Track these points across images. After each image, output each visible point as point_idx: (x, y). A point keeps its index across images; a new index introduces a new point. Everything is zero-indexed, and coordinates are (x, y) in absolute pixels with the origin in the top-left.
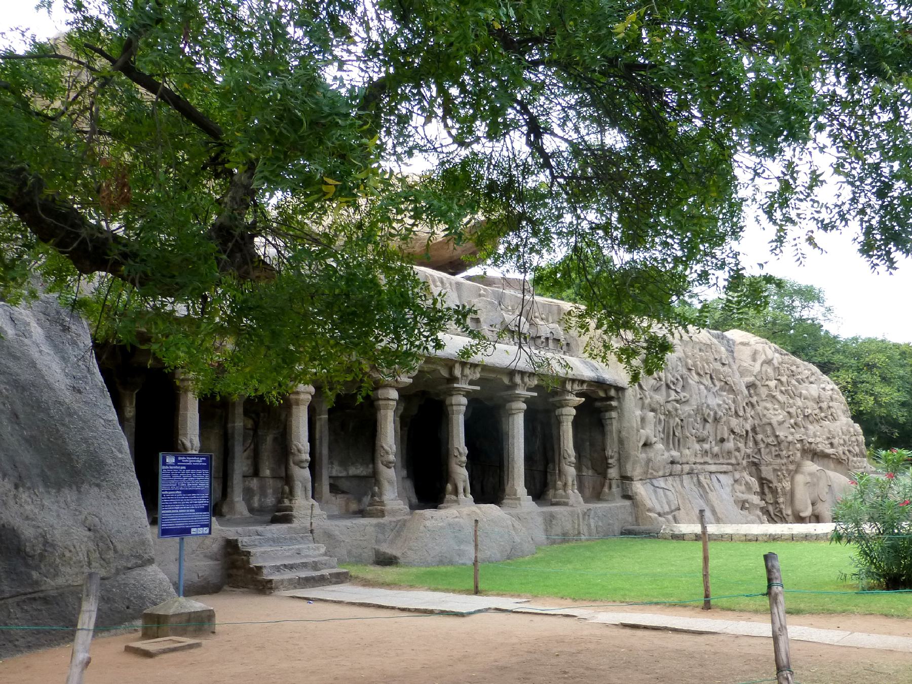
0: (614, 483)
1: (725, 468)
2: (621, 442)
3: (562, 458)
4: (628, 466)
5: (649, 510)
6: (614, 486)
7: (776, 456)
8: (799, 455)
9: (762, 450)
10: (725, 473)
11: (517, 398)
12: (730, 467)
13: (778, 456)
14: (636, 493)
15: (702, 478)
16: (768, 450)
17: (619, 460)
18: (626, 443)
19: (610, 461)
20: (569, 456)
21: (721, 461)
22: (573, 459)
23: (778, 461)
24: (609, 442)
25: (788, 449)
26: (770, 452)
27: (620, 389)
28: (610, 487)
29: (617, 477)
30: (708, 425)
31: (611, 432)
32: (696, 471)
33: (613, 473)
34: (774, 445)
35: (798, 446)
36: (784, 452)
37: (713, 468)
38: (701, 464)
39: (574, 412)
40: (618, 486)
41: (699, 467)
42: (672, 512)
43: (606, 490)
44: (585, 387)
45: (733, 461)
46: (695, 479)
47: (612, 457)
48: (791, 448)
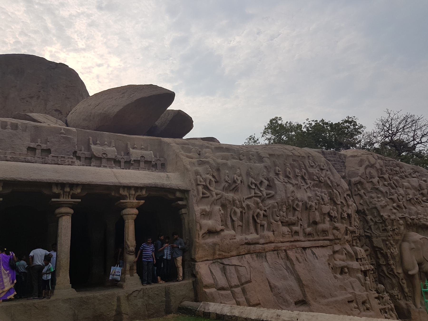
1: (321, 243)
5: (207, 287)
7: (383, 230)
8: (402, 228)
9: (372, 227)
10: (322, 247)
11: (60, 205)
12: (327, 243)
13: (385, 230)
14: (197, 272)
15: (290, 253)
16: (377, 226)
21: (316, 238)
22: (132, 249)
23: (385, 234)
25: (393, 225)
26: (378, 228)
27: (185, 192)
30: (297, 213)
32: (284, 248)
34: (381, 223)
35: (401, 222)
36: (389, 227)
37: (307, 244)
38: (291, 242)
39: (135, 211)
41: (288, 244)
42: (242, 284)
44: (144, 192)
45: (331, 237)
46: (283, 255)
48: (395, 223)
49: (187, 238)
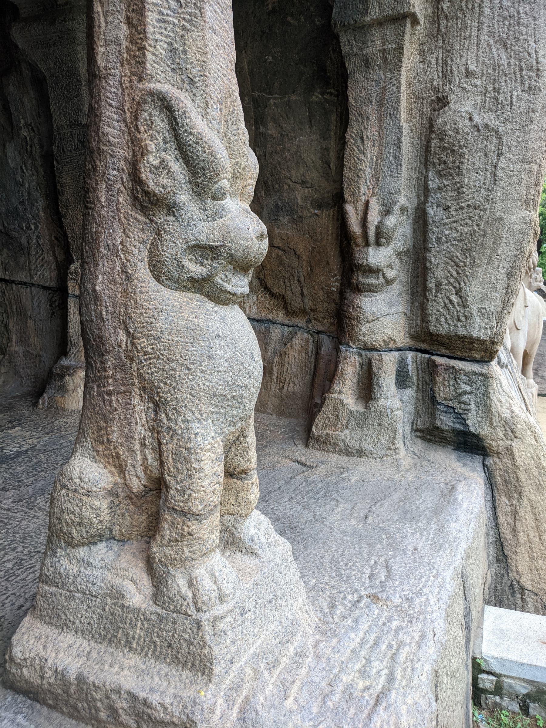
0: (388, 364)
2: (437, 152)
3: (111, 195)
4: (474, 290)
6: (387, 380)
14: (510, 428)
17: (418, 260)
18: (472, 160)
19: (376, 256)
20: (201, 176)
24: (365, 159)
28: (367, 389)
29: (402, 339)
31: (387, 107)
33: (383, 314)
40: (402, 379)
43: (345, 393)
47: (381, 238)
49: (402, 200)
